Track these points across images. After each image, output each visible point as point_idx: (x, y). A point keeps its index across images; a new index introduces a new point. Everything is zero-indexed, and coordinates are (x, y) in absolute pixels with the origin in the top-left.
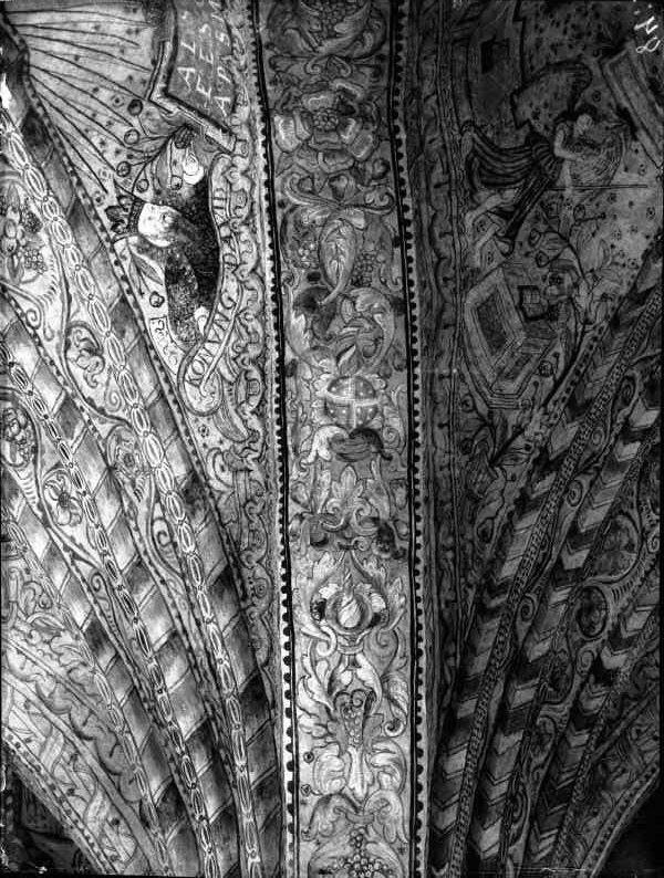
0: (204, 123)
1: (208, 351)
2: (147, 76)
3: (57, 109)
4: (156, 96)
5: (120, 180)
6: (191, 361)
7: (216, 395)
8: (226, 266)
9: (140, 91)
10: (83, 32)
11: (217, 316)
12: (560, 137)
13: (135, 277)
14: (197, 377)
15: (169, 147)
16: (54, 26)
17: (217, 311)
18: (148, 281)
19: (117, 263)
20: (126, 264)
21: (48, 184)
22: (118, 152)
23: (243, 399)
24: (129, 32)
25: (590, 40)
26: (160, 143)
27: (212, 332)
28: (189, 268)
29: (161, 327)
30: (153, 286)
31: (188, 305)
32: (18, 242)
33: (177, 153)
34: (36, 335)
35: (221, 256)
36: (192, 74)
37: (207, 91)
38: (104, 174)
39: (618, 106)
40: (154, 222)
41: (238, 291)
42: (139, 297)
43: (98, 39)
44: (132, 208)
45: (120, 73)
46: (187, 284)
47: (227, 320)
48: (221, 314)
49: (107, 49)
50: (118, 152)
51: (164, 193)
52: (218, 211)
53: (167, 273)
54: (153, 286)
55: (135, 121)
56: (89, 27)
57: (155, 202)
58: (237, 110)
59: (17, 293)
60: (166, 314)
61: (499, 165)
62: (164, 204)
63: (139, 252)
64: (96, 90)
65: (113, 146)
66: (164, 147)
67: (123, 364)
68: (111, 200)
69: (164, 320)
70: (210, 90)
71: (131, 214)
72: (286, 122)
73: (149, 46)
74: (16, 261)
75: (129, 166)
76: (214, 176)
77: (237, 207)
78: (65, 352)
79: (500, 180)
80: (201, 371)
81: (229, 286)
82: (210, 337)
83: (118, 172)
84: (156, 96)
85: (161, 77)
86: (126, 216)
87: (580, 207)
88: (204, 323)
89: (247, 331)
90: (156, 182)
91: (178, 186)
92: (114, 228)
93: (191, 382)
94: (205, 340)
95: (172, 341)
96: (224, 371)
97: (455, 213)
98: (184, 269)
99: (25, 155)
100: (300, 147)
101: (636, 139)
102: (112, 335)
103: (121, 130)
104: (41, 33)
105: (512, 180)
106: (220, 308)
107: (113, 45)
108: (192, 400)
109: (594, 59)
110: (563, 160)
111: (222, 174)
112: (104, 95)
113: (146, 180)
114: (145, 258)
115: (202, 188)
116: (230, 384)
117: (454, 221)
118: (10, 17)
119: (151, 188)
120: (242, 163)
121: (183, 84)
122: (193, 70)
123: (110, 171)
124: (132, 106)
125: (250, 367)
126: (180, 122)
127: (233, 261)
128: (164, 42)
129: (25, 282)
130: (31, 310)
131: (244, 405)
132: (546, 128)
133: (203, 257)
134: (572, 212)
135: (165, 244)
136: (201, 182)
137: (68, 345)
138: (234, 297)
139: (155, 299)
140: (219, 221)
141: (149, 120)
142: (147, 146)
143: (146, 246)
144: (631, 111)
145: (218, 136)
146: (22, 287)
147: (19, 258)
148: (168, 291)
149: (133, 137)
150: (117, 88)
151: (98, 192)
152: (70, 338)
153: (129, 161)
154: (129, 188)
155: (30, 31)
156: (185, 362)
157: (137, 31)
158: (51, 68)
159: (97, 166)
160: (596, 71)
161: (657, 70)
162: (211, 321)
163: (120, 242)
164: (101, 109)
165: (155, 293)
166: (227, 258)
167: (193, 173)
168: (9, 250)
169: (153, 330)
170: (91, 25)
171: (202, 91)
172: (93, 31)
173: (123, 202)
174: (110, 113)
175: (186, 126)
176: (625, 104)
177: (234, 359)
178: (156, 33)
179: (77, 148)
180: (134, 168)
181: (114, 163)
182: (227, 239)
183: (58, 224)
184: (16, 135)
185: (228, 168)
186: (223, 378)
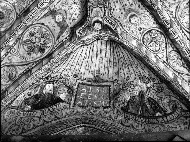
0: (74, 97)
1: (21, 113)
2: (82, 78)
3: (74, 55)
4: (78, 81)
5: (58, 77)
6: (17, 109)
7: (11, 120)
8: (43, 111)
9: (79, 76)
10: (92, 59)
11: (30, 112)
13: (34, 87)
14: (13, 113)
15: (67, 88)
16: (93, 51)
17: (31, 112)
18: (34, 90)
19: (37, 81)
20: (37, 83)
21: (57, 62)
22: (65, 75)
23: (13, 129)
24: (92, 71)
26: (68, 85)
27: (26, 112)
28: (39, 100)
29: (23, 97)
30: (33, 92)
31: (30, 103)
32: (35, 43)
33: (66, 91)
34: (8, 53)
35: (45, 109)
36: (84, 91)
37: (82, 97)
38: (59, 72)
40: (49, 88)
41: (38, 116)
42: (29, 89)
43: (90, 63)
44: (51, 81)
45: (82, 70)
46: (35, 101)
47: (30, 116)
48: (31, 113)
49: (88, 65)
50: (65, 75)
51: (56, 89)
52: (56, 107)
53: (37, 95)
54: (33, 92)
55: (72, 77)
56: (93, 61)
57: (54, 87)
58: (80, 108)
59: (19, 43)
60: (26, 98)
62: (54, 90)
63: (41, 86)
64: (78, 64)
65: (66, 73)
66: (67, 87)
67: (13, 96)
68: (53, 75)
69: (25, 97)
70: (82, 98)
71: (50, 81)
72: (83, 129)
73: (89, 77)
74: (29, 43)
75: (62, 78)
76: (63, 103)
77: (58, 113)
78: (6, 66)
80: (15, 113)
81: (38, 113)
82: (24, 112)
83: (60, 76)
84: (78, 81)
85: (82, 82)
86: (49, 80)
88: (27, 109)
89: (29, 123)
90: (59, 86)
91: (59, 93)
92: (46, 77)
93: (11, 111)
94: (23, 111)
95: (20, 102)
96: (18, 120)
98: (39, 99)
99: (64, 54)
100: (78, 132)
102: (20, 90)
103: (70, 74)
104: (92, 48)
106: (32, 112)
107: (88, 66)
108: (7, 113)
111: (64, 106)
112: (77, 67)
113: (59, 83)
114: (39, 88)
115: (60, 100)
116: (15, 123)
118: (96, 41)
119: (57, 85)
120: (68, 111)
121: (82, 89)
122: (85, 91)
123: (60, 74)
124: (75, 75)
125: (21, 128)
126: (73, 89)
127: (45, 113)
128: (90, 82)
129: (23, 47)
130: (15, 50)
131: (12, 130)
133: (43, 104)
135: (44, 93)
136: (61, 99)
137: (8, 66)
138: (36, 116)
139: (29, 93)
140: (54, 107)
141: (72, 80)
142: (67, 82)
143: (43, 88)
145: (73, 102)
146: (22, 45)
147: (30, 44)
148: (32, 97)
149: (68, 78)
150: (79, 70)
151: (54, 72)
152: (11, 67)
153: (63, 78)
154: (56, 79)
155: (92, 46)
156: (16, 108)
157: (92, 74)
158: (83, 51)
159: (61, 70)
162: (28, 111)
163: (43, 80)
164: (74, 67)
165: (31, 93)
166: (44, 111)
167: (62, 96)
168: (32, 39)
169: (21, 95)
170: (93, 61)
171: (81, 95)
172: (92, 62)
173: (53, 78)
174: (73, 70)
175: (73, 92)
177: (21, 122)
178: (92, 79)
179: (65, 64)
180: (61, 80)
181: (62, 75)
182: (49, 110)
183: (47, 67)
184: (69, 51)
185: (66, 107)
186: (16, 120)
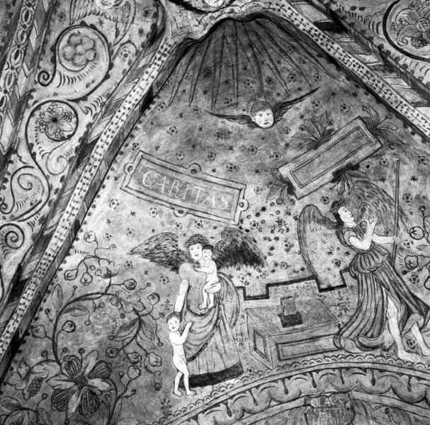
12: (354, 241)
25: (282, 209)
39: (333, 181)
61: (368, 314)
79: (379, 315)
87: (412, 232)
97: (395, 369)
101: (357, 167)
105: (381, 303)
109: (297, 202)
110: (372, 242)
117: (402, 371)
132: (347, 253)
134: (415, 241)
144: (334, 170)
160: (306, 201)
161: (300, 144)
176: (329, 176)
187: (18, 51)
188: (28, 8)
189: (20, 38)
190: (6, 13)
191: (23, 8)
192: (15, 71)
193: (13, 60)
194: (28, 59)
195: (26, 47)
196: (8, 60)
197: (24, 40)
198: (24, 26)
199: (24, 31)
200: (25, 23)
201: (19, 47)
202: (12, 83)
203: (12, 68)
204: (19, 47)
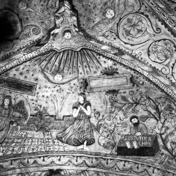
187: (162, 14)
188: (150, 2)
189: (158, 11)
190: (148, 12)
191: (149, 4)
192: (169, 19)
193: (165, 17)
194: (167, 11)
195: (163, 10)
196: (164, 19)
197: (160, 9)
198: (155, 7)
199: (157, 8)
200: (154, 6)
201: (161, 13)
202: (173, 22)
203: (167, 19)
204: (161, 13)
